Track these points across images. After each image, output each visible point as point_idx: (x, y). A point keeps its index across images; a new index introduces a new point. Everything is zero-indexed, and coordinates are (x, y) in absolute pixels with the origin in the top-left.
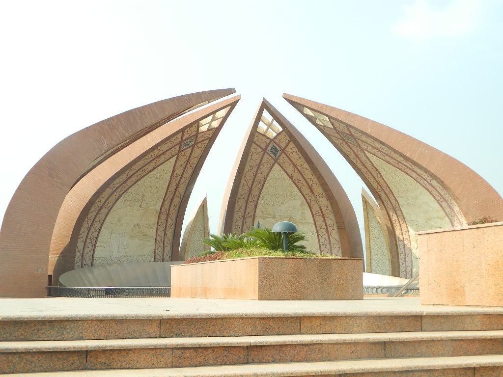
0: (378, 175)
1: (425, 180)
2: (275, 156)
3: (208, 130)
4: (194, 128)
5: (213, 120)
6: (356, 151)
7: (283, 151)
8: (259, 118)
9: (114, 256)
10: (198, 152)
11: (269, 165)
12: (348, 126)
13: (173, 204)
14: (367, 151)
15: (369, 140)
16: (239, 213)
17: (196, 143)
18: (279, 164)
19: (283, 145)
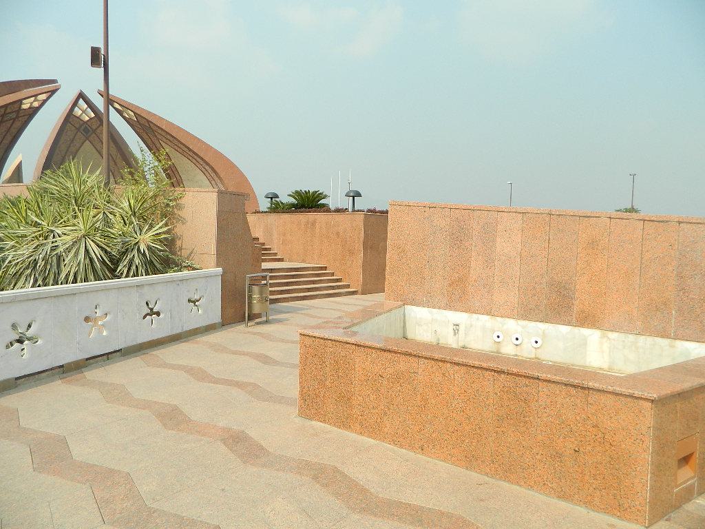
3: (30, 108)
4: (16, 106)
5: (34, 101)
7: (94, 131)
8: (75, 104)
10: (18, 124)
12: (148, 121)
15: (164, 134)
17: (17, 117)
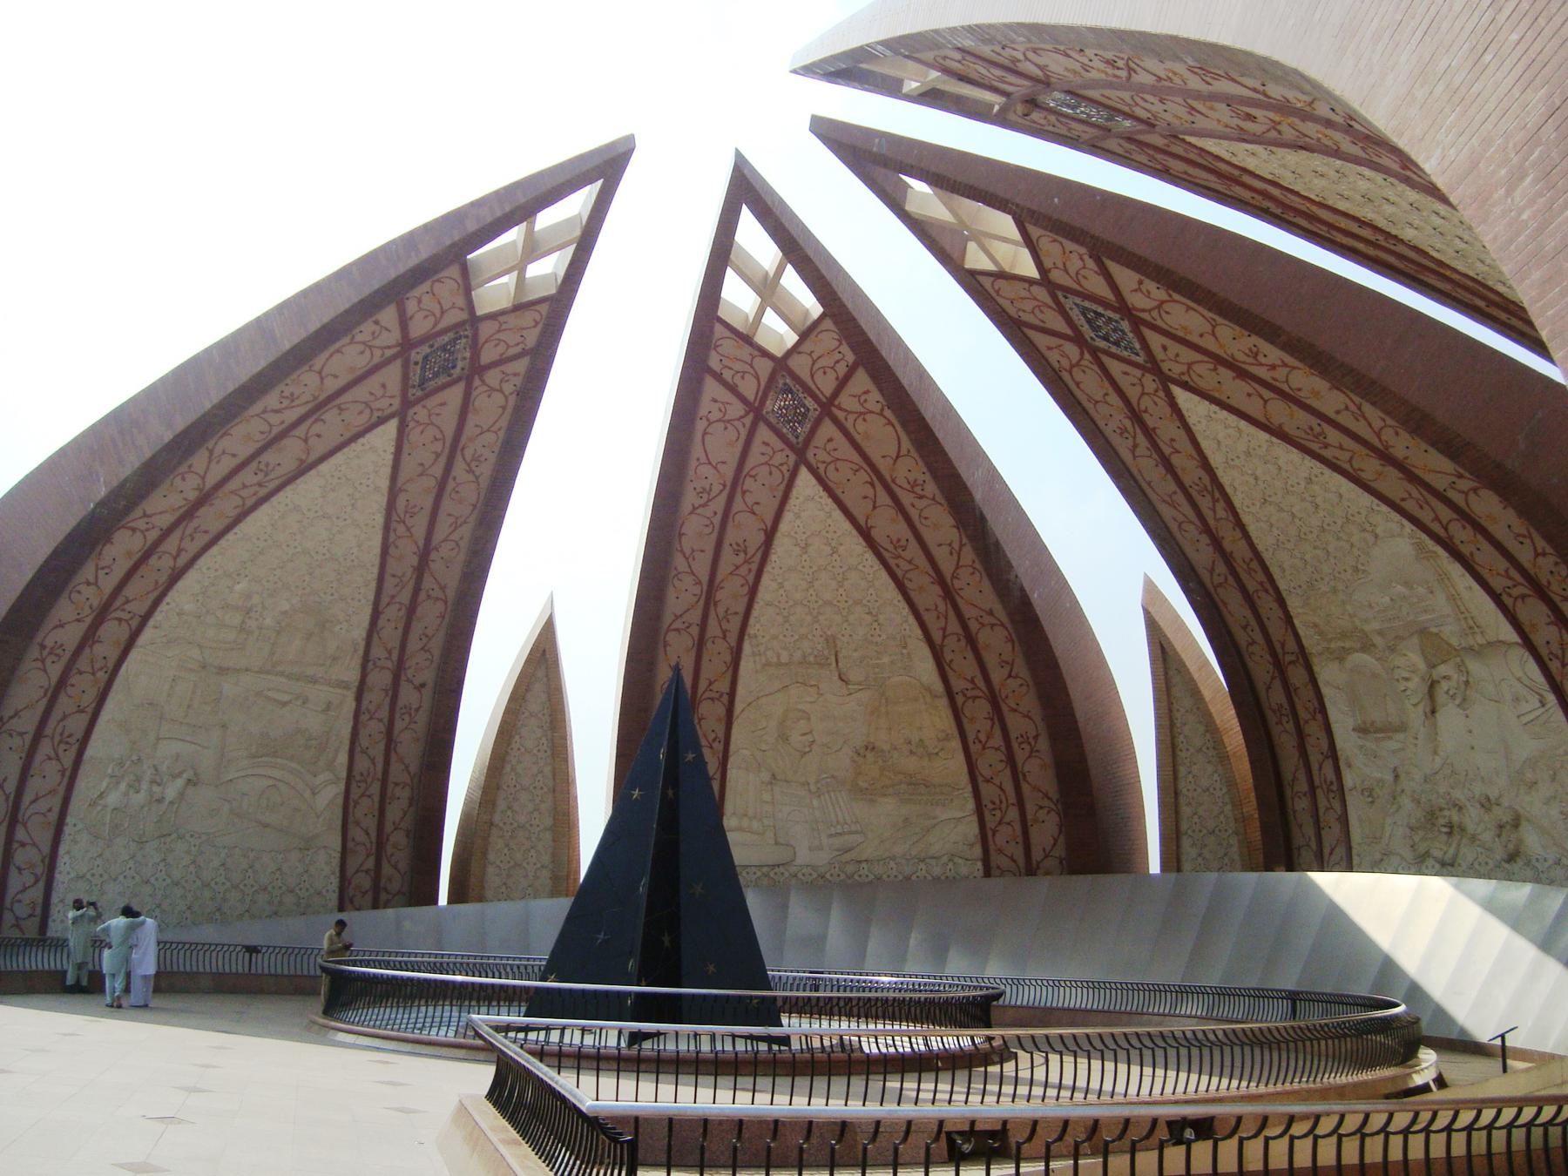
3: (804, 335)
7: (1124, 309)
9: (798, 861)
13: (991, 660)
18: (1185, 386)
19: (1098, 286)
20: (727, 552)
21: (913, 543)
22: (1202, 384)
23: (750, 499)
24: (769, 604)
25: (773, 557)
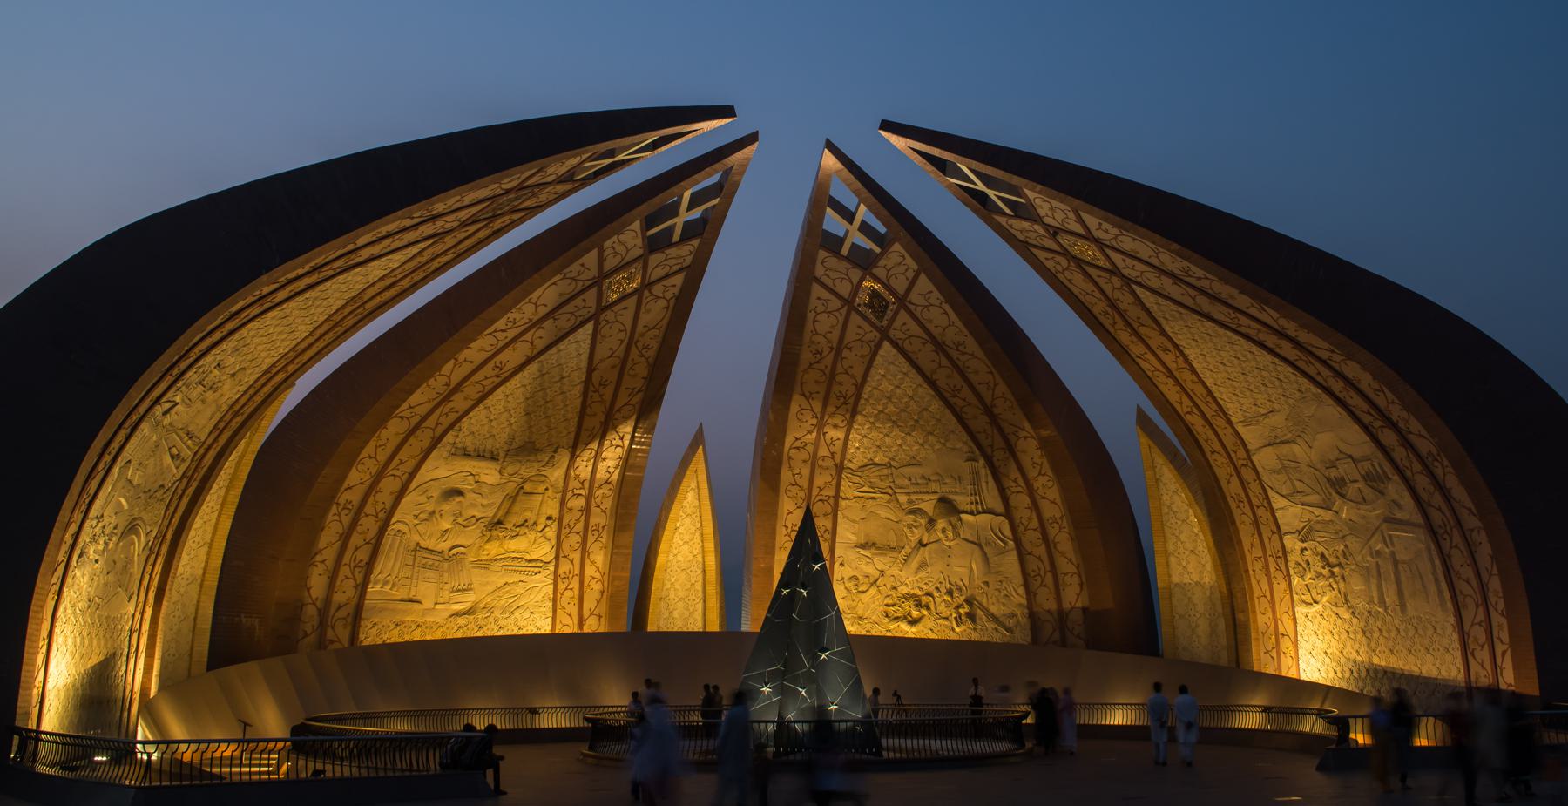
0: (1181, 360)
1: (1324, 362)
2: (881, 319)
6: (1108, 288)
7: (902, 301)
11: (866, 350)
14: (1140, 284)
16: (795, 490)
18: (895, 344)
19: (900, 285)
20: (491, 364)
21: (613, 386)
22: (907, 346)
23: (540, 333)
24: (487, 408)
25: (518, 377)
